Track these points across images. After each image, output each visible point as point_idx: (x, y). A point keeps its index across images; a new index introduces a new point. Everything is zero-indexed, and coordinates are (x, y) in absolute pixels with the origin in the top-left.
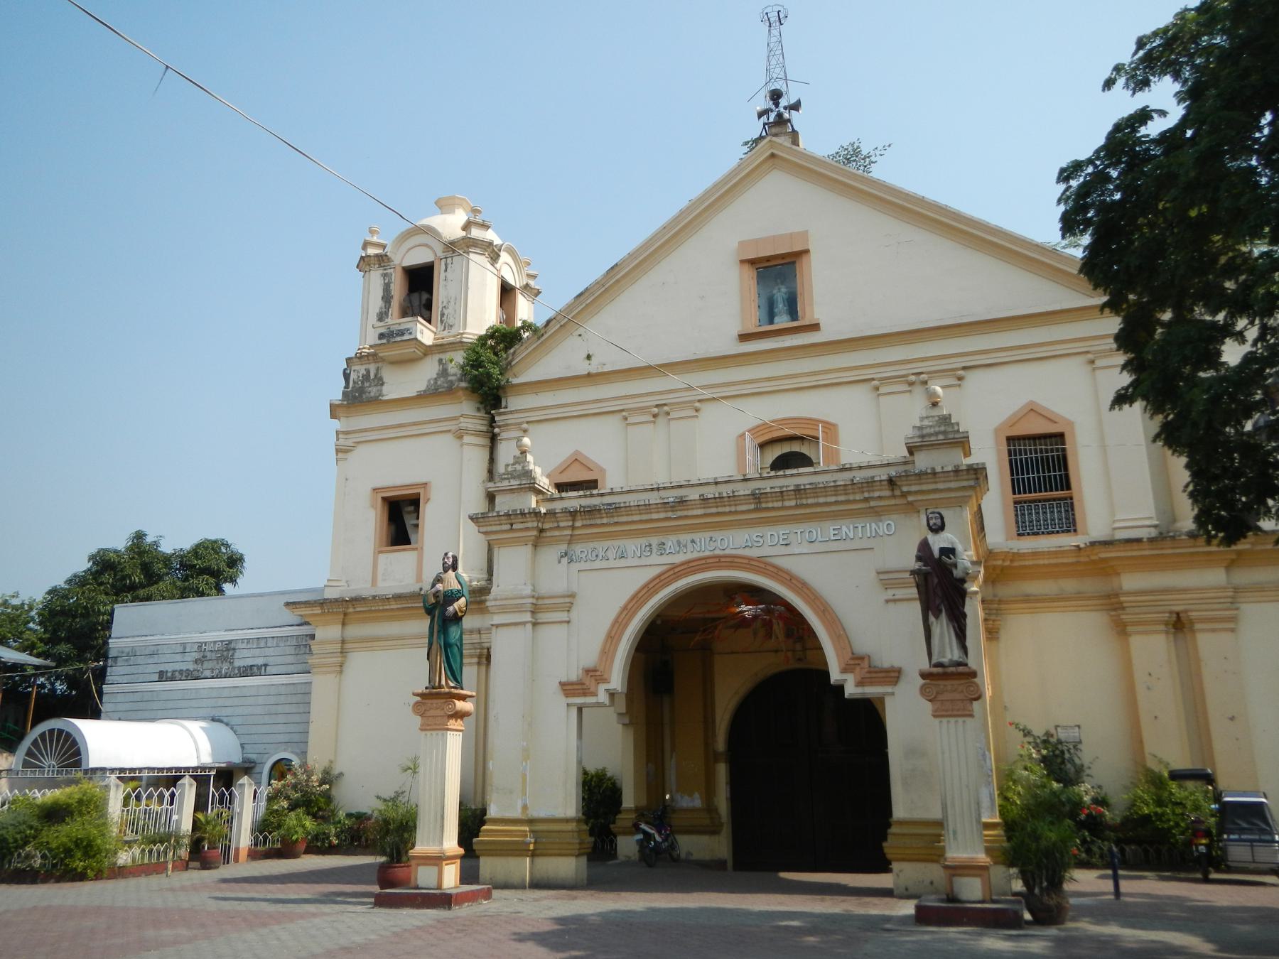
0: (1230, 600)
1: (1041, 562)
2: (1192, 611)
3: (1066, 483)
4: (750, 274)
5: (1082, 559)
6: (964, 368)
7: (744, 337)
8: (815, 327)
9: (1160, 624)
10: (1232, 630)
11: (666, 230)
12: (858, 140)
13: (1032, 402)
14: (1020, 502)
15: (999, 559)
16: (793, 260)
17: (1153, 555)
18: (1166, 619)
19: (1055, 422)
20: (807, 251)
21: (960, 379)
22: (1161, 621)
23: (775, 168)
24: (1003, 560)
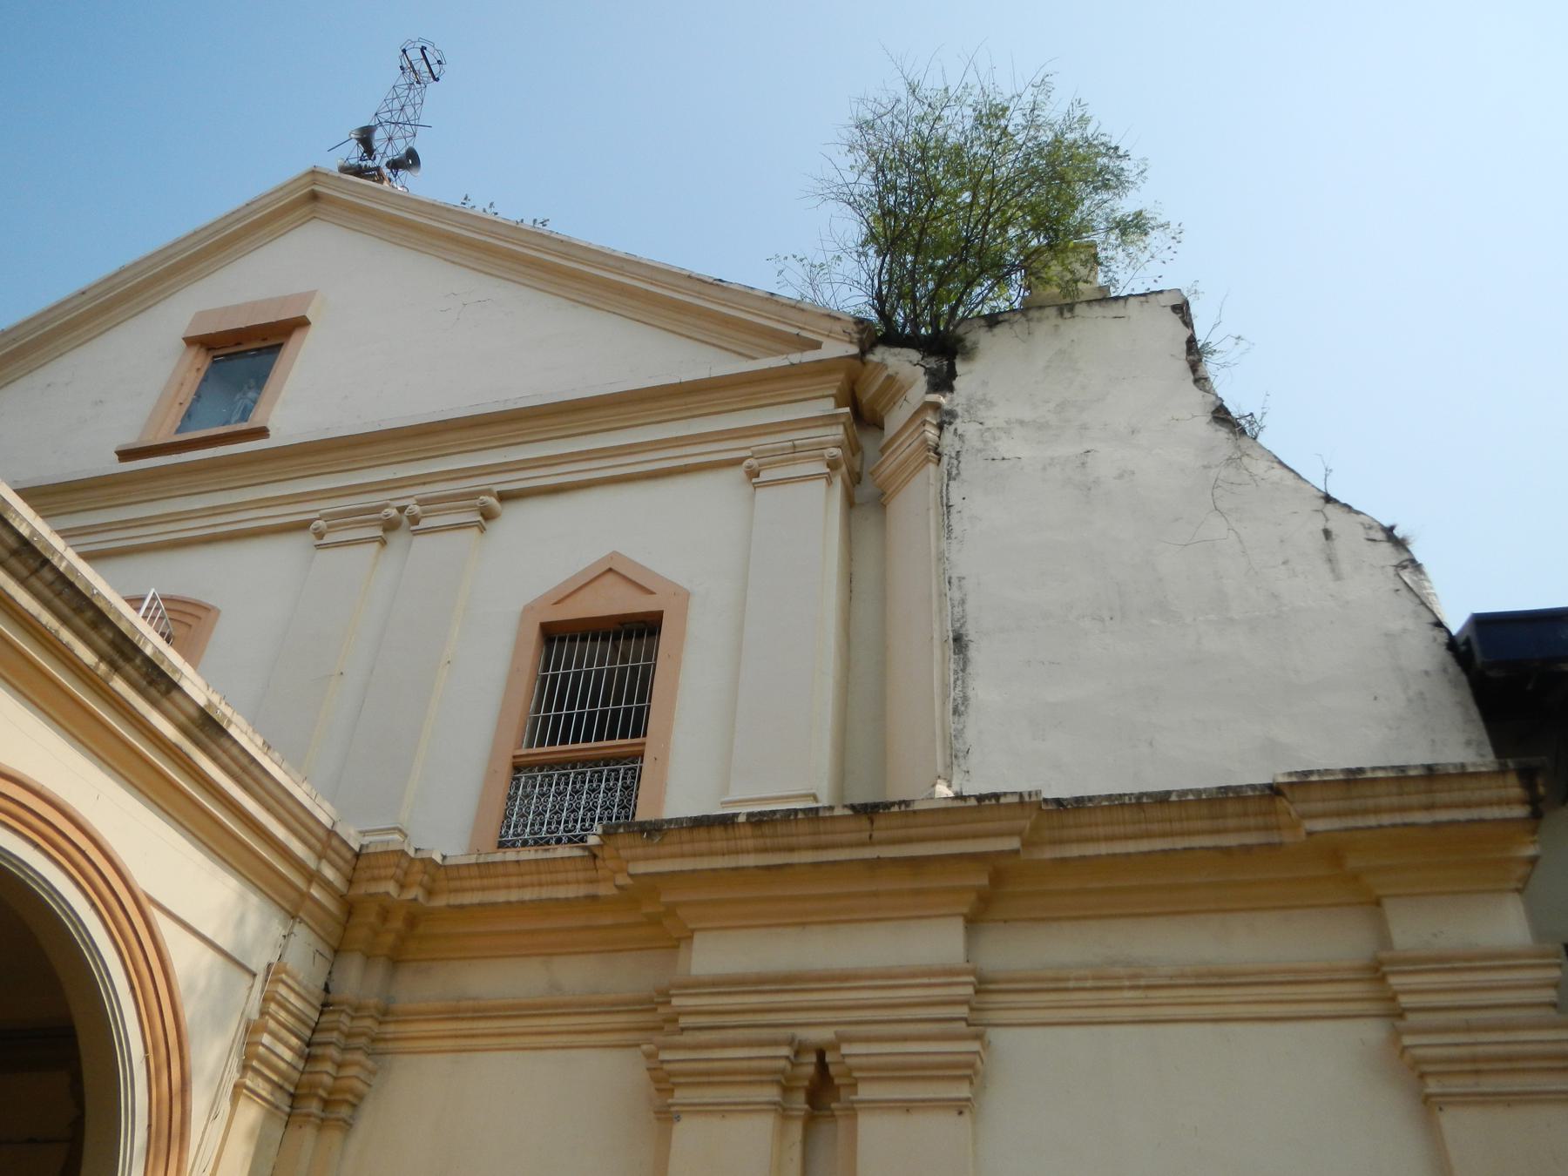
0: (963, 1011)
1: (501, 896)
2: (851, 1040)
3: (637, 724)
4: (200, 361)
5: (604, 890)
6: (504, 497)
7: (125, 455)
8: (262, 433)
9: (762, 1083)
10: (961, 1107)
11: (84, 297)
12: (491, 205)
13: (614, 555)
14: (530, 767)
15: (386, 878)
16: (278, 342)
17: (768, 868)
18: (782, 1063)
19: (652, 593)
20: (301, 323)
21: (488, 515)
22: (760, 1072)
23: (315, 217)
24: (402, 886)
